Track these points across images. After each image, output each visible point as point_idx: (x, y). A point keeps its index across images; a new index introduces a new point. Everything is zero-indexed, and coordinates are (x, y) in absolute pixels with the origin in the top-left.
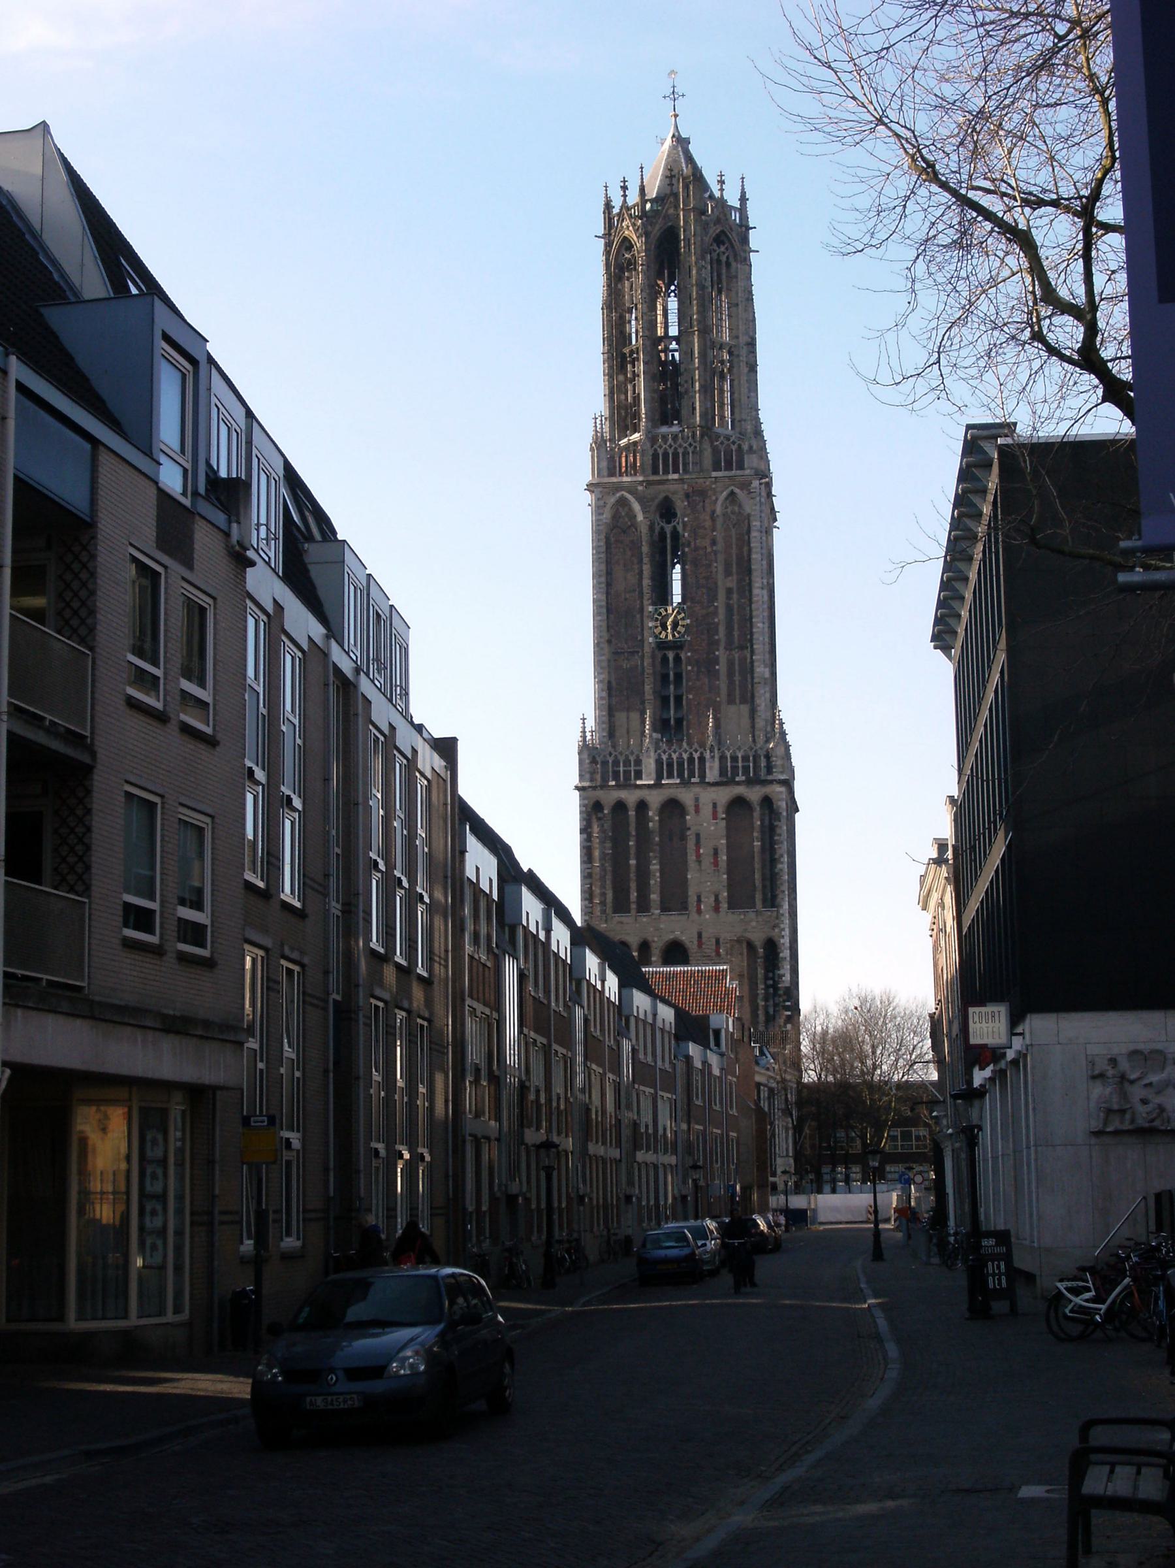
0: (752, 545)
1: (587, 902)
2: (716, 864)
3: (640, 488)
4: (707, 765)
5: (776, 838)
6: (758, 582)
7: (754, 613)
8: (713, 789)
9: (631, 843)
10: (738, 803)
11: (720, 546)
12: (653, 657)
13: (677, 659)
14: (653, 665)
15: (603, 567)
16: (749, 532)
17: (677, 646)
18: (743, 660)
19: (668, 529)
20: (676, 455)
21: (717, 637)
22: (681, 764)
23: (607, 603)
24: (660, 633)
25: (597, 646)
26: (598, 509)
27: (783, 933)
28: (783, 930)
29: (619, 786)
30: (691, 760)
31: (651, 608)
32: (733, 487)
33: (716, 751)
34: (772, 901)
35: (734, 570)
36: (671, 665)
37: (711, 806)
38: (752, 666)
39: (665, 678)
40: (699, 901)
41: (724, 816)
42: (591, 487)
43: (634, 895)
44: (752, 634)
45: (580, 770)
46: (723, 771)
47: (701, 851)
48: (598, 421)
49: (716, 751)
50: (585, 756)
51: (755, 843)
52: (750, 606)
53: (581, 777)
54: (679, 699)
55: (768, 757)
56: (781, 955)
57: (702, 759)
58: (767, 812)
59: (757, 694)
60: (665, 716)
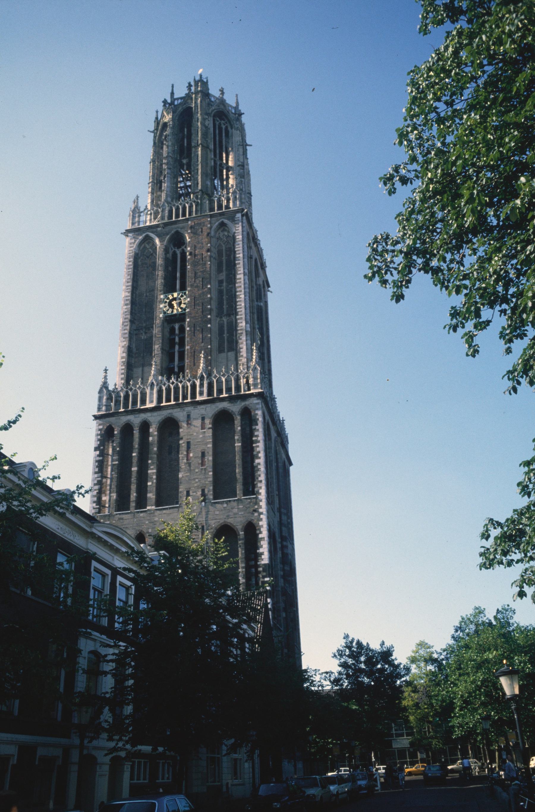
0: (236, 249)
1: (94, 505)
4: (198, 389)
8: (203, 406)
9: (134, 454)
17: (181, 318)
19: (178, 252)
24: (168, 310)
27: (262, 516)
29: (127, 413)
31: (162, 297)
36: (177, 332)
39: (172, 343)
40: (188, 494)
43: (133, 495)
47: (191, 455)
51: (236, 445)
56: (260, 536)
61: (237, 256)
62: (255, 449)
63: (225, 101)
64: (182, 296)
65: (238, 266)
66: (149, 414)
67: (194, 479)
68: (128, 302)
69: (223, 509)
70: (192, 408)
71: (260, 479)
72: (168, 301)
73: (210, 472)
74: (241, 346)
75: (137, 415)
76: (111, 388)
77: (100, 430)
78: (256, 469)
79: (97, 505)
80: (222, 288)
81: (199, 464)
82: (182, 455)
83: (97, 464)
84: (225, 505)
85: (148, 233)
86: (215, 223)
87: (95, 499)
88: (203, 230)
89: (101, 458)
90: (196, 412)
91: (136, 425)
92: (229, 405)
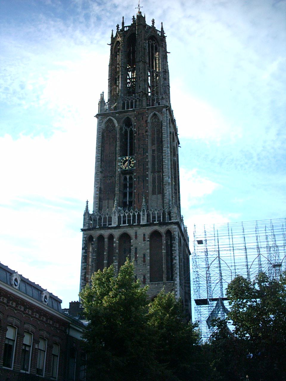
0: (163, 132)
1: (83, 281)
2: (144, 261)
3: (117, 115)
4: (141, 217)
5: (173, 248)
6: (167, 150)
7: (164, 157)
8: (144, 228)
9: (105, 253)
10: (155, 235)
11: (149, 133)
12: (120, 177)
13: (131, 178)
14: (120, 179)
15: (100, 144)
16: (161, 128)
17: (130, 172)
18: (159, 177)
20: (132, 103)
21: (147, 167)
22: (129, 221)
23: (101, 157)
25: (96, 173)
26: (99, 124)
27: (177, 293)
28: (177, 291)
29: (101, 228)
30: (134, 216)
31: (119, 158)
32: (155, 112)
33: (145, 212)
34: (171, 278)
35: (156, 142)
37: (143, 235)
38: (163, 178)
39: (125, 186)
41: (148, 239)
42: (97, 116)
44: (163, 165)
45: (84, 223)
46: (148, 220)
47: (138, 256)
48: (102, 95)
49: (145, 212)
50: (87, 216)
51: (163, 251)
52: (162, 155)
53: (84, 225)
54: (131, 194)
55: (169, 213)
57: (139, 216)
58: (169, 238)
59: (165, 189)
60: (124, 200)
61: (164, 136)
62: (173, 254)
63: (155, 28)
64: (131, 159)
65: (164, 142)
66: (113, 230)
67: (140, 270)
68: (99, 160)
69: (155, 287)
70: (138, 228)
71: (176, 272)
72: (123, 161)
73: (148, 266)
74: (165, 192)
75: (106, 231)
76: (91, 212)
77: (85, 238)
78: (174, 266)
79: (84, 281)
80: (154, 155)
81: (142, 261)
82: (133, 256)
83: (83, 257)
84: (156, 286)
85: (110, 117)
86: (150, 114)
87: (83, 278)
88: (144, 118)
89: (86, 254)
90: (141, 231)
91: (106, 236)
92: (159, 228)
